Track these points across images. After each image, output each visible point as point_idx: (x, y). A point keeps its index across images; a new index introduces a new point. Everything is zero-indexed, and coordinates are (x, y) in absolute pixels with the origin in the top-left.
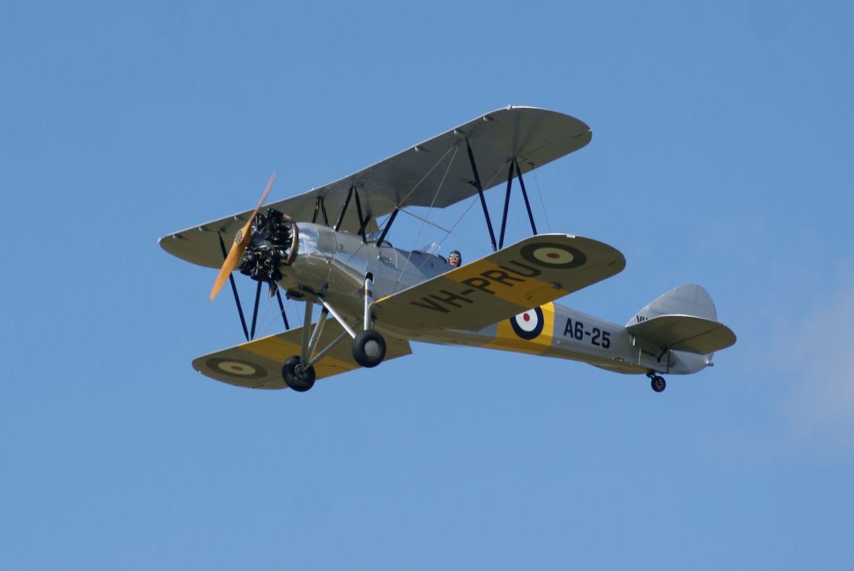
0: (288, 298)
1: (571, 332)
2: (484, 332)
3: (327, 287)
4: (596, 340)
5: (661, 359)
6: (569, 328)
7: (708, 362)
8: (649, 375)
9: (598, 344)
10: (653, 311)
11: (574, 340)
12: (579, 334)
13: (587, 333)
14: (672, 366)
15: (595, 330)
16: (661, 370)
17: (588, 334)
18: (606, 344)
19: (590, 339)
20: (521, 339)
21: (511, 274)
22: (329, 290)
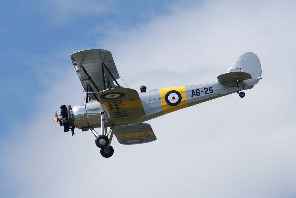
0: (83, 132)
1: (194, 94)
3: (88, 124)
4: (206, 93)
6: (193, 94)
7: (259, 78)
9: (208, 93)
10: (231, 70)
11: (197, 97)
12: (198, 94)
13: (202, 92)
15: (205, 89)
16: (238, 90)
17: (203, 92)
18: (211, 91)
19: (204, 93)
20: (173, 106)
22: (90, 124)
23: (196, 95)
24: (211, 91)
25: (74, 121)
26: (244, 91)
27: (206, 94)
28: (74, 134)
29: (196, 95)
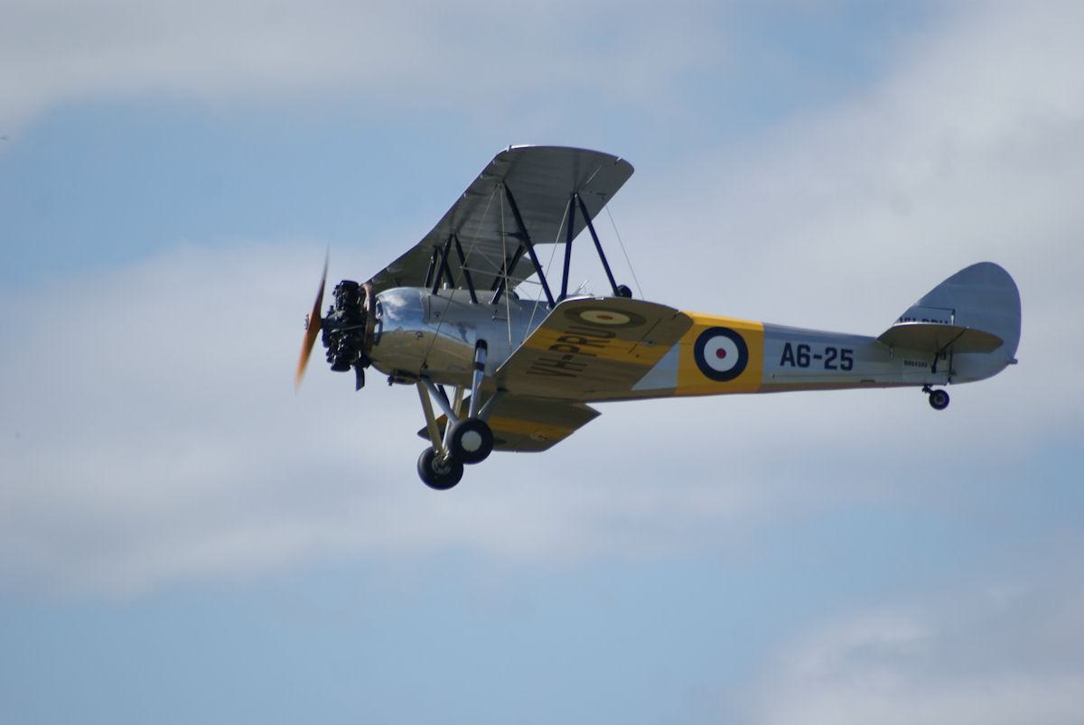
0: (390, 384)
1: (791, 359)
2: (637, 387)
3: (425, 366)
4: (831, 363)
5: (937, 366)
6: (788, 356)
8: (926, 390)
9: (835, 368)
11: (797, 369)
12: (803, 360)
14: (952, 377)
15: (828, 350)
17: (818, 357)
19: (822, 362)
21: (589, 338)
22: (429, 369)
23: (796, 360)
24: (846, 363)
25: (377, 343)
26: (948, 388)
27: (827, 366)
28: (363, 385)
29: (796, 360)
